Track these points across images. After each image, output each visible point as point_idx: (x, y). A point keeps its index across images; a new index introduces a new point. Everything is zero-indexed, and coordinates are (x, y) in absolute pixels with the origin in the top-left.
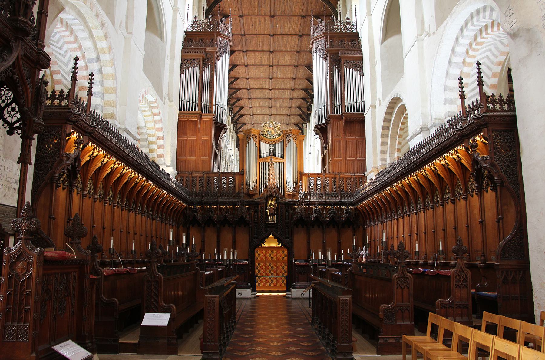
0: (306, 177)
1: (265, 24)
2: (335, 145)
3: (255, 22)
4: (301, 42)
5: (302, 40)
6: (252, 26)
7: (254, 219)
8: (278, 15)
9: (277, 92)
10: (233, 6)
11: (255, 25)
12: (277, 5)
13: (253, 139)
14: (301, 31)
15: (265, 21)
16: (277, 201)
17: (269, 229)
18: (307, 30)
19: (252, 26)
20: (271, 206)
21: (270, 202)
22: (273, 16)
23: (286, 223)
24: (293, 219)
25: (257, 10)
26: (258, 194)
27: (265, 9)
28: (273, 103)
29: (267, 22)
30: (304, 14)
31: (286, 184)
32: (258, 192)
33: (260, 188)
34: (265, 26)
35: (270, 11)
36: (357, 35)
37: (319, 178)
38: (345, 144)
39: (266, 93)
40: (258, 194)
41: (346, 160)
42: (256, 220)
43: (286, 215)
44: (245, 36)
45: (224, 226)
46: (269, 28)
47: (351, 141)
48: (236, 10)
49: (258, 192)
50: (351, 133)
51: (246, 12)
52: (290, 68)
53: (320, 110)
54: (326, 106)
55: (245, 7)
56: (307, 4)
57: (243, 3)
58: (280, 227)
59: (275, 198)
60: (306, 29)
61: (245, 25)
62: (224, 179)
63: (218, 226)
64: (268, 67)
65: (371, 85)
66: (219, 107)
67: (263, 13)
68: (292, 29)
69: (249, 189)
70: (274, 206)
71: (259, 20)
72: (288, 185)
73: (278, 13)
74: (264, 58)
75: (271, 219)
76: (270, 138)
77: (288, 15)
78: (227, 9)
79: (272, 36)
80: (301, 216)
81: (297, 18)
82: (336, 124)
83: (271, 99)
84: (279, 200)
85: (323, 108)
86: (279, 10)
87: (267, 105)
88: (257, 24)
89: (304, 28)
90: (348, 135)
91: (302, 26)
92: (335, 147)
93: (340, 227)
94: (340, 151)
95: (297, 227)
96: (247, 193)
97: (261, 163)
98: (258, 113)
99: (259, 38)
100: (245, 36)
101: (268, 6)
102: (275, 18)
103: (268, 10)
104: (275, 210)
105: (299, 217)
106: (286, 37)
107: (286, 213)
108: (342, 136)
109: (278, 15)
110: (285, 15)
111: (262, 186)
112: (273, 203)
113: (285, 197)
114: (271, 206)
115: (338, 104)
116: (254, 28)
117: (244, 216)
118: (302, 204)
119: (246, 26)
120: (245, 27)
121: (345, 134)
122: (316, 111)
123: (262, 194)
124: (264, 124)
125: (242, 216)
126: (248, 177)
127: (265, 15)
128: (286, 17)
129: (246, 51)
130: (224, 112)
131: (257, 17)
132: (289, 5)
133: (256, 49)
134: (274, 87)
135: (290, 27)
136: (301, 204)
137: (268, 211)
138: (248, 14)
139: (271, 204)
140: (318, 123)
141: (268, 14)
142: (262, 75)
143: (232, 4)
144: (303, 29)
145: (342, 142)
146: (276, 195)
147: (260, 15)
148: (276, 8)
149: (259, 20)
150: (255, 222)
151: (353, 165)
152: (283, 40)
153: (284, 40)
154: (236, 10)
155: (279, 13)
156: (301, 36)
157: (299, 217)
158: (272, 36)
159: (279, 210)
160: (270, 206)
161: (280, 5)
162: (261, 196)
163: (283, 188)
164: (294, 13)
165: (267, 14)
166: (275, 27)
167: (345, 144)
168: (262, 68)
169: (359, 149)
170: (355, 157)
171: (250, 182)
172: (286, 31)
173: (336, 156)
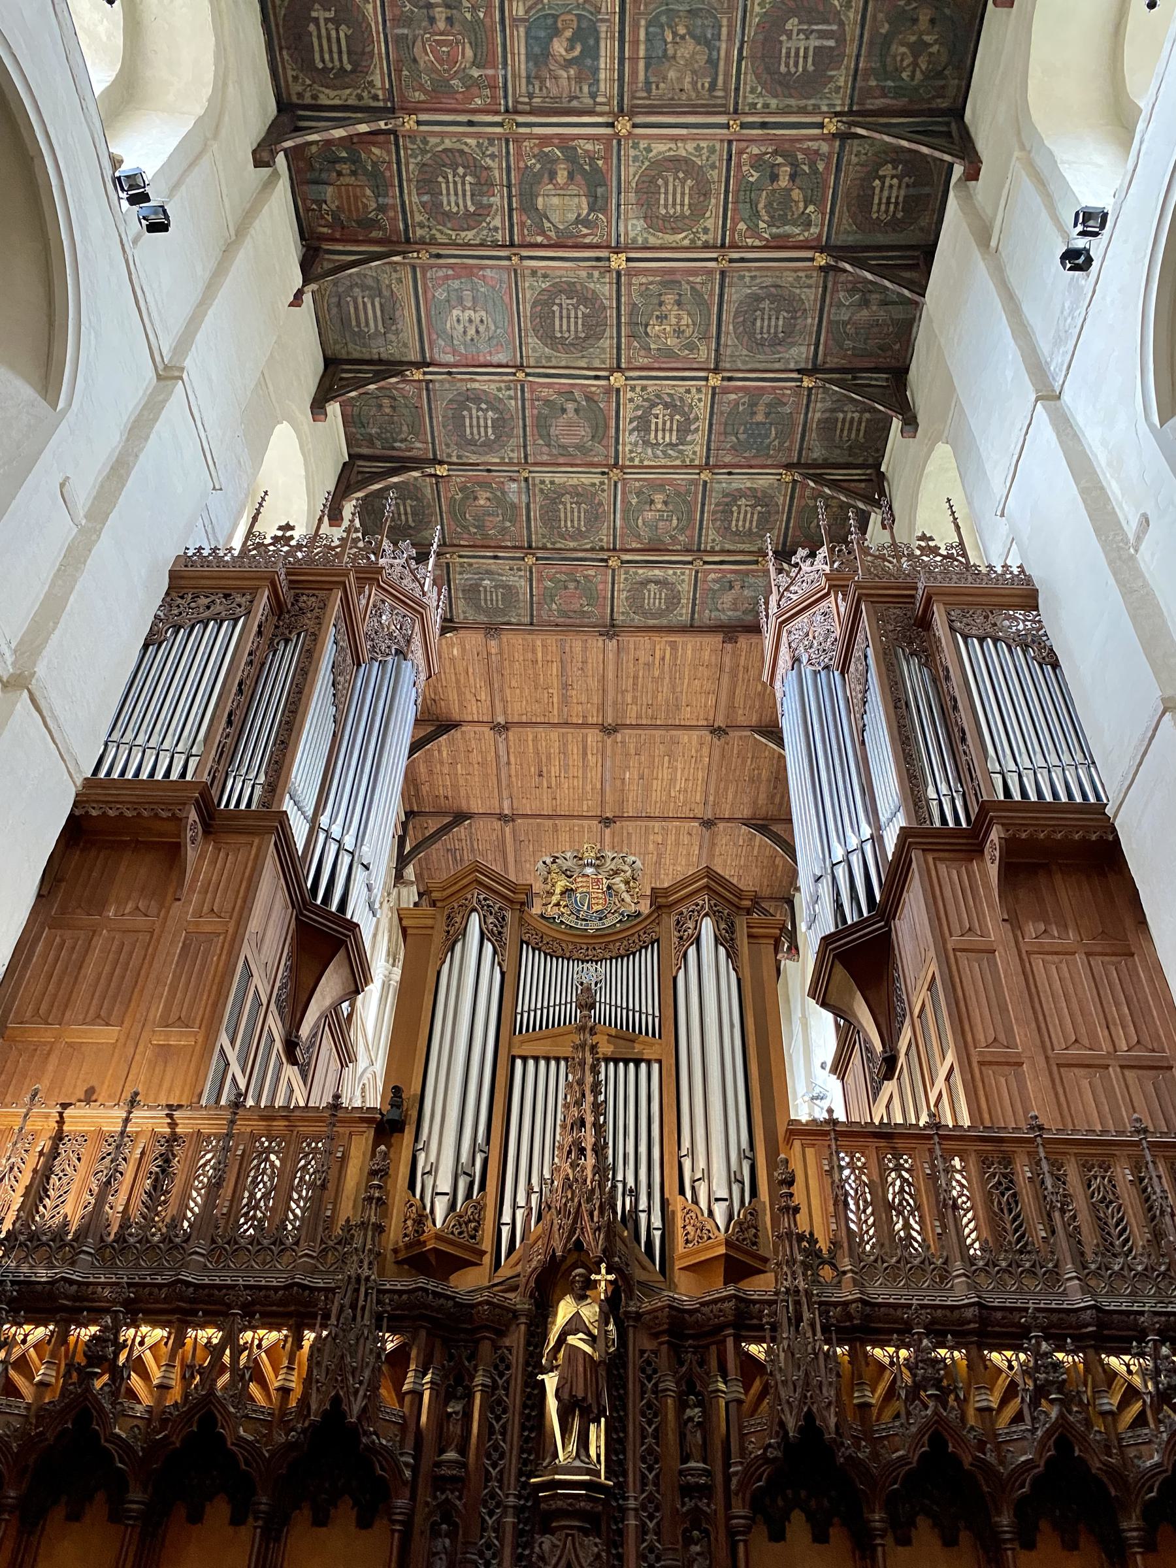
0: (810, 1152)
1: (585, 767)
2: (967, 981)
3: (549, 758)
4: (713, 845)
5: (713, 836)
6: (540, 775)
7: (442, 1451)
8: (631, 727)
10: (472, 681)
11: (549, 772)
12: (627, 677)
13: (483, 920)
14: (711, 798)
15: (585, 754)
16: (611, 1307)
17: (547, 1541)
18: (730, 796)
19: (540, 775)
20: (572, 1340)
21: (565, 1309)
22: (609, 730)
23: (687, 1491)
24: (743, 1450)
25: (555, 700)
26: (487, 1259)
27: (584, 699)
29: (590, 756)
30: (720, 723)
31: (682, 1192)
32: (487, 1245)
33: (507, 1218)
34: (584, 778)
35: (602, 708)
37: (897, 1156)
38: (1027, 975)
40: (487, 1259)
41: (1047, 1058)
42: (451, 1455)
43: (683, 1423)
44: (513, 820)
45: (196, 1517)
46: (599, 786)
47: (1056, 958)
48: (483, 698)
49: (487, 1245)
50: (1047, 922)
51: (518, 709)
53: (841, 872)
54: (868, 847)
55: (514, 684)
56: (734, 675)
57: (506, 663)
58: (643, 1530)
59: (603, 1278)
60: (726, 789)
61: (513, 773)
62: (269, 1150)
63: (136, 1499)
65: (1134, 618)
66: (333, 847)
68: (679, 792)
69: (422, 1218)
70: (592, 1340)
72: (695, 1201)
75: (572, 1447)
76: (581, 925)
78: (453, 696)
79: (607, 822)
80: (809, 1416)
81: (695, 734)
82: (949, 873)
84: (630, 1297)
85: (855, 859)
86: (634, 702)
88: (555, 771)
89: (722, 785)
90: (1031, 929)
91: (714, 776)
92: (970, 992)
93: (1131, 1525)
94: (1003, 1009)
95: (777, 1535)
96: (408, 1246)
97: (519, 1062)
100: (513, 820)
101: (594, 684)
102: (619, 737)
104: (602, 1372)
105: (791, 1423)
107: (682, 1405)
108: (994, 929)
109: (631, 727)
110: (656, 727)
111: (515, 1206)
112: (590, 1312)
113: (672, 1286)
114: (572, 1340)
115: (944, 789)
116: (545, 785)
117: (356, 1409)
118: (806, 1315)
119: (517, 776)
120: (514, 779)
121: (1013, 921)
122: (818, 879)
123: (515, 1256)
124: (549, 860)
125: (336, 1401)
126: (427, 1143)
127: (585, 725)
128: (658, 733)
130: (359, 875)
131: (554, 734)
132: (667, 676)
135: (672, 781)
136: (799, 1318)
137: (551, 1382)
138: (524, 719)
139: (575, 1325)
140: (837, 927)
141: (595, 721)
143: (471, 670)
144: (717, 792)
145: (1006, 961)
146: (608, 1253)
147: (566, 724)
148: (622, 692)
150: (444, 1471)
151: (1100, 1090)
152: (647, 843)
153: (651, 847)
154: (483, 698)
155: (634, 715)
156: (708, 824)
157: (791, 1423)
158: (607, 822)
159: (632, 1373)
160: (561, 1340)
161: (636, 677)
162: (505, 1272)
163: (657, 1222)
164: (686, 715)
165: (590, 721)
166: (618, 783)
167: (1027, 975)
169: (1117, 1005)
170: (1106, 1047)
171: (432, 1171)
173: (981, 1037)
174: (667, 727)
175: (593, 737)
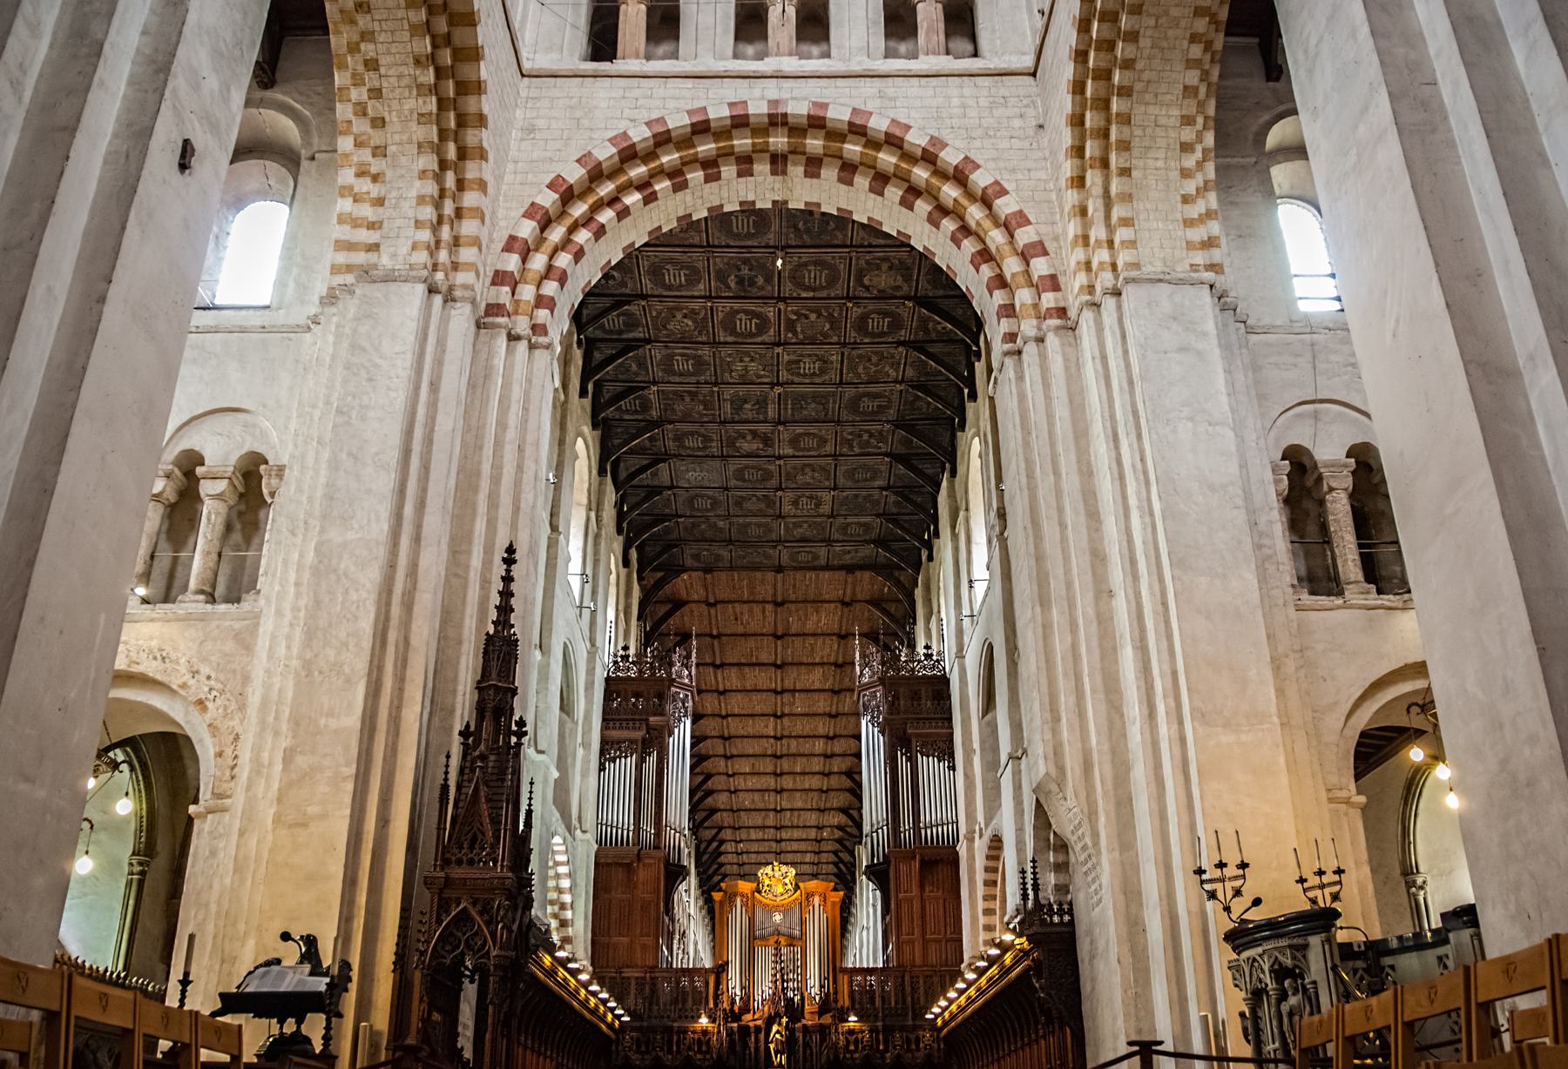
9: (794, 743)
21: (775, 1028)
28: (785, 765)
36: (944, 681)
39: (768, 746)
52: (822, 696)
64: (772, 696)
67: (760, 598)
71: (751, 611)
73: (793, 597)
74: (763, 678)
77: (814, 601)
83: (781, 757)
87: (770, 769)
98: (750, 785)
99: (751, 643)
103: (771, 591)
106: (811, 640)
129: (722, 665)
133: (743, 661)
134: (786, 733)
142: (758, 709)
149: (751, 611)
161: (794, 586)
168: (756, 697)
172: (810, 626)
174: (814, 601)
175: (769, 607)
